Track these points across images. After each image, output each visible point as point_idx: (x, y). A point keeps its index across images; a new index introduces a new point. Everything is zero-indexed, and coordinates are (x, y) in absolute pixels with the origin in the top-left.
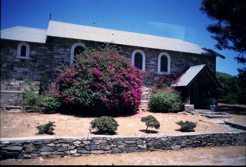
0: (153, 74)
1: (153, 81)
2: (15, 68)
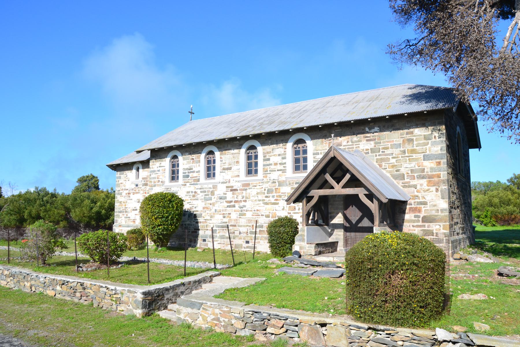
0: (276, 181)
1: (277, 196)
2: (131, 195)
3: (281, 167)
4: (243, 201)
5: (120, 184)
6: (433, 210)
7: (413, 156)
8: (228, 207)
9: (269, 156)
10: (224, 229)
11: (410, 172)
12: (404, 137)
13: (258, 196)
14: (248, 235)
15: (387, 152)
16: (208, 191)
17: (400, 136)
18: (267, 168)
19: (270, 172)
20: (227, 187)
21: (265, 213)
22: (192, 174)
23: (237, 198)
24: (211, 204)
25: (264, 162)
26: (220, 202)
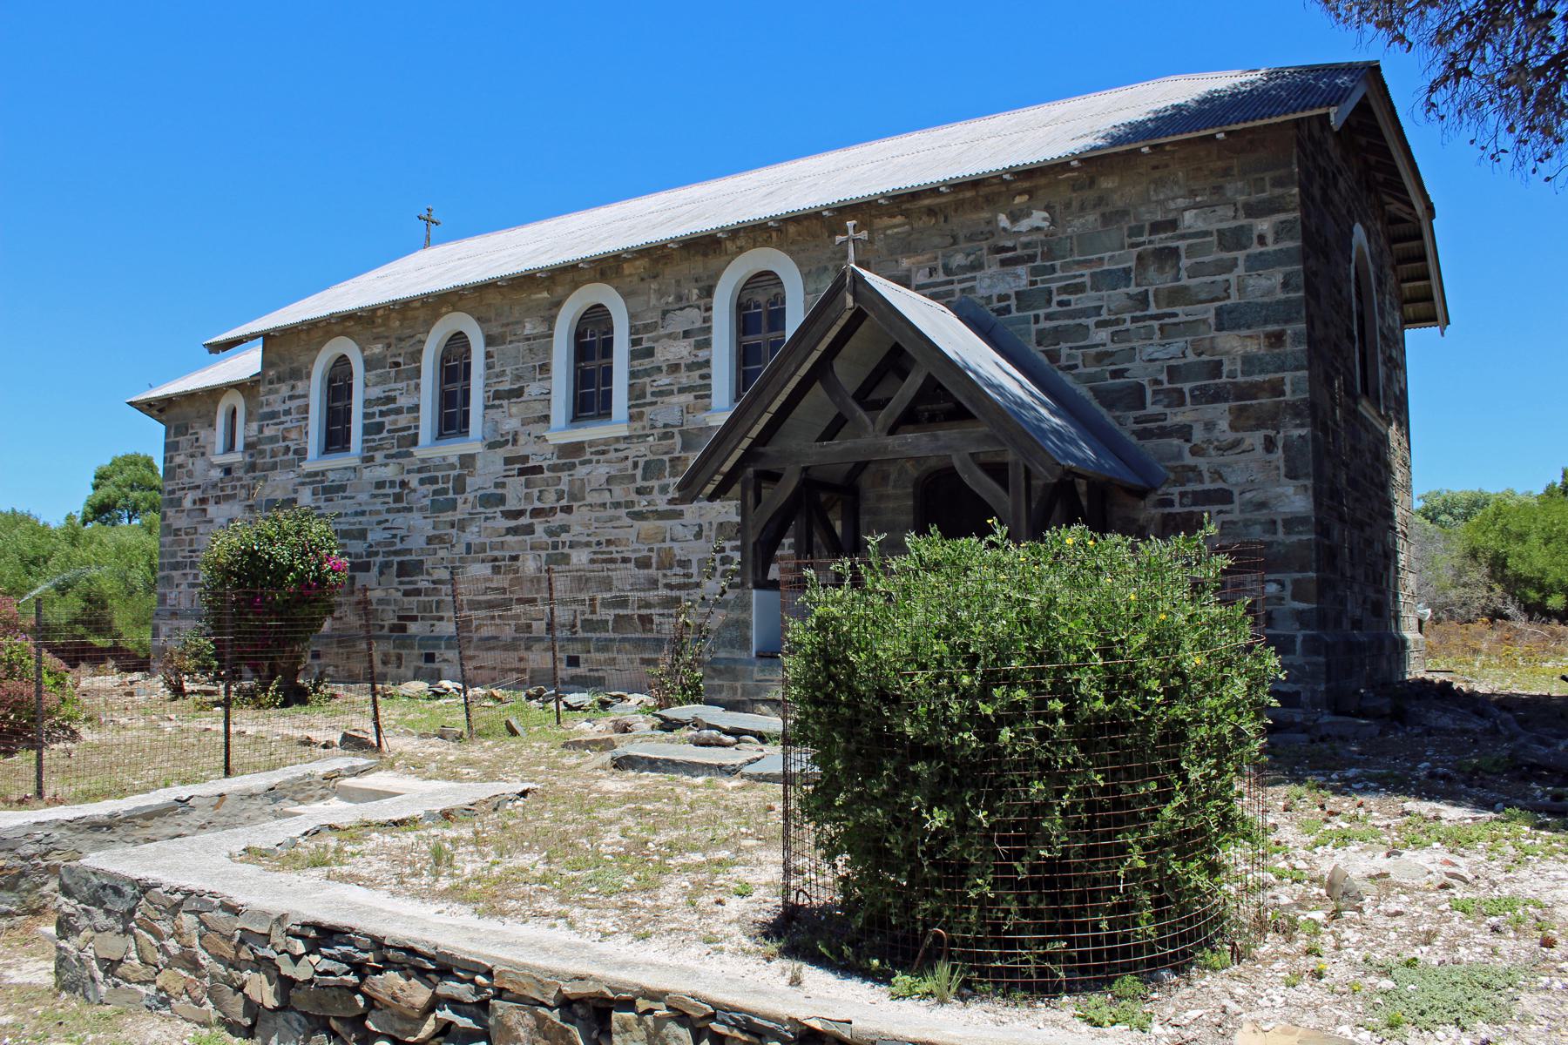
0: (675, 430)
2: (212, 509)
3: (694, 378)
5: (174, 468)
6: (1255, 522)
7: (1175, 315)
8: (509, 531)
9: (649, 339)
11: (1164, 377)
12: (1144, 243)
13: (610, 490)
14: (576, 633)
15: (1078, 301)
16: (446, 479)
17: (1127, 241)
18: (645, 383)
19: (654, 399)
22: (392, 417)
24: (453, 526)
25: (635, 363)
26: (483, 516)
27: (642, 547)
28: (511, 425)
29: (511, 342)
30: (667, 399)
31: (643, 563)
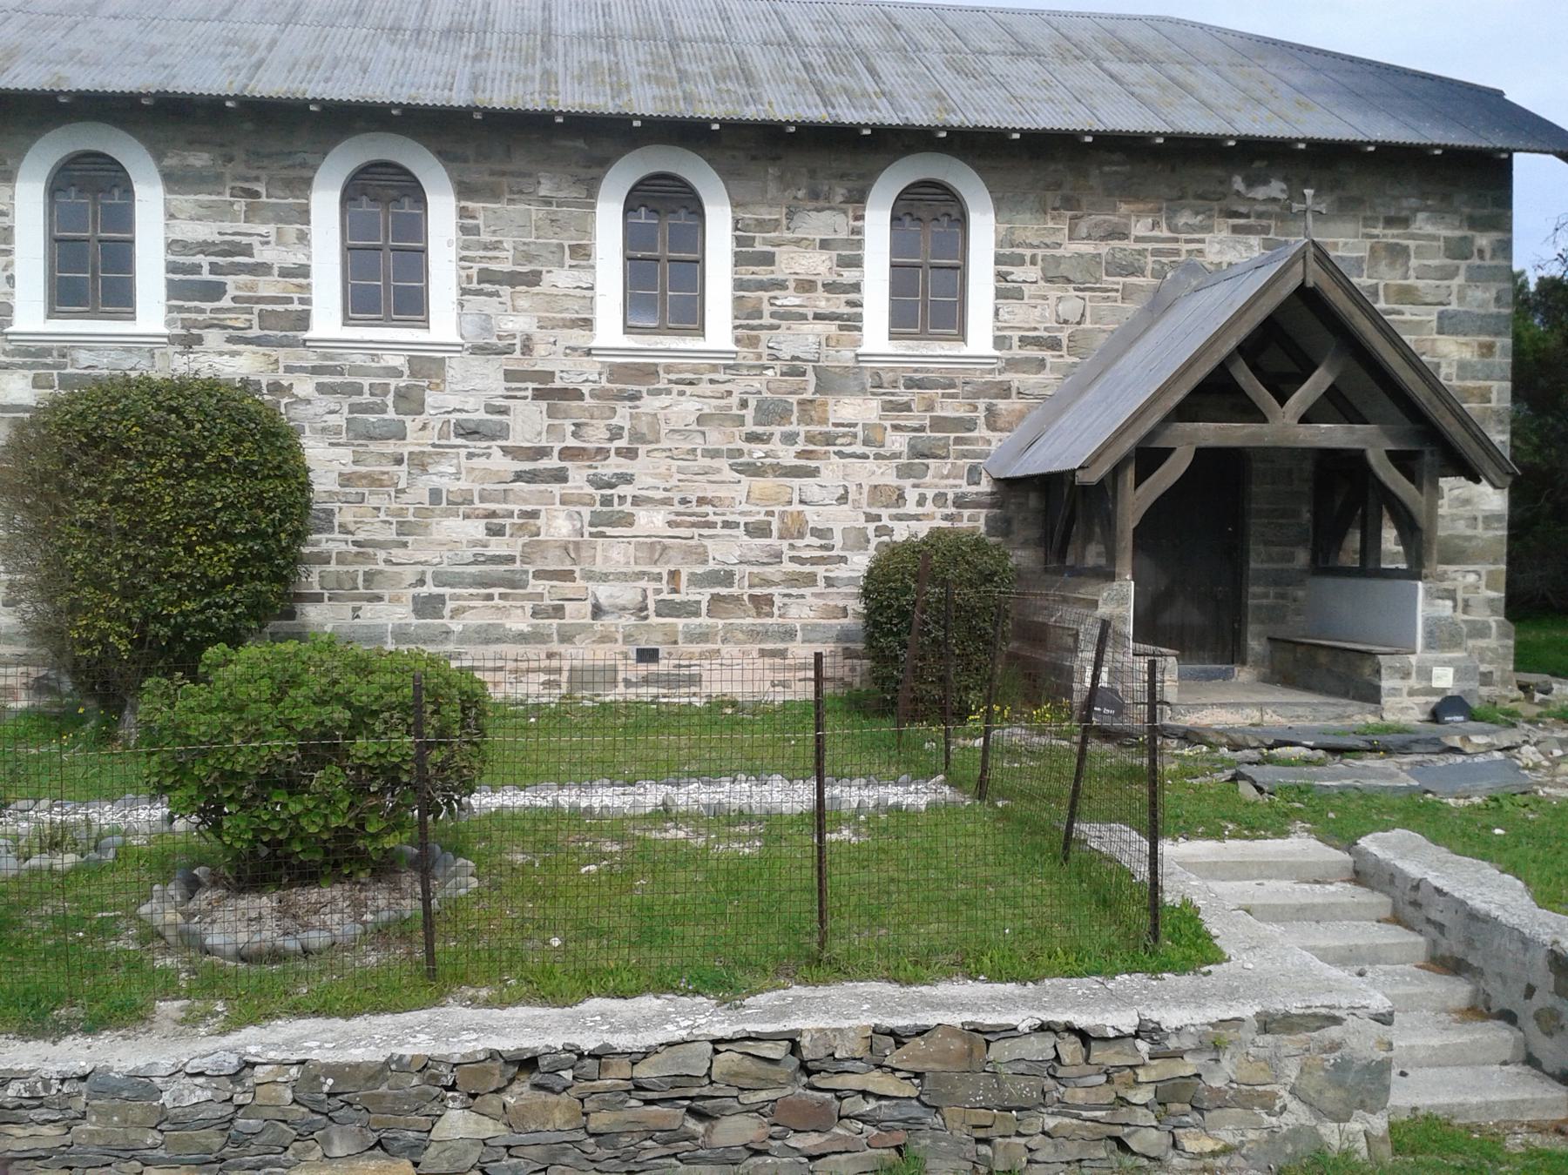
0: (809, 367)
1: (810, 439)
3: (838, 304)
4: (619, 452)
6: (1461, 518)
7: (1400, 313)
8: (519, 476)
9: (765, 242)
10: (496, 591)
12: (1377, 236)
14: (646, 618)
18: (760, 299)
20: (510, 375)
21: (741, 513)
23: (574, 434)
26: (463, 452)
27: (754, 509)
28: (517, 324)
29: (511, 201)
30: (795, 325)
31: (759, 530)
